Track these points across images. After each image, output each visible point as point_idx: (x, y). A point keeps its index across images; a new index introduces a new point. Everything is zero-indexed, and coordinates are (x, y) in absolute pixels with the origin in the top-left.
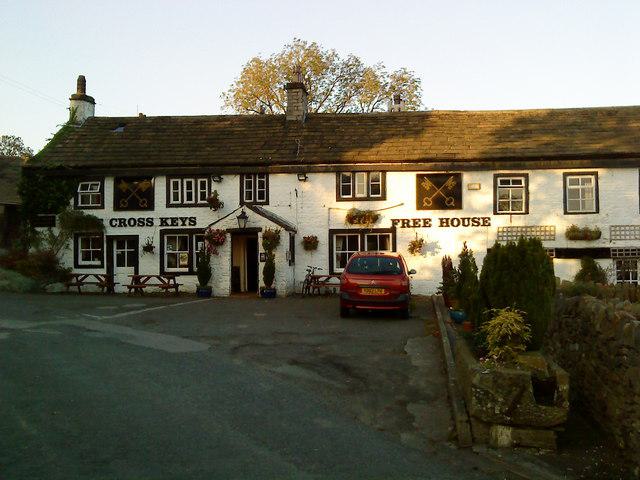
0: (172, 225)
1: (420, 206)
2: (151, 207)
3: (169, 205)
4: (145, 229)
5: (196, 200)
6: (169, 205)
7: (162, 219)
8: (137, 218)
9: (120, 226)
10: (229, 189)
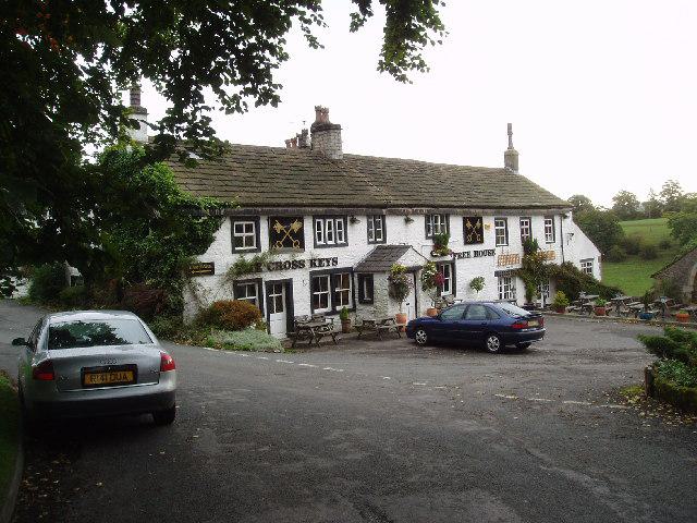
1: (466, 243)
2: (302, 246)
3: (316, 246)
4: (297, 270)
6: (316, 246)
10: (358, 232)
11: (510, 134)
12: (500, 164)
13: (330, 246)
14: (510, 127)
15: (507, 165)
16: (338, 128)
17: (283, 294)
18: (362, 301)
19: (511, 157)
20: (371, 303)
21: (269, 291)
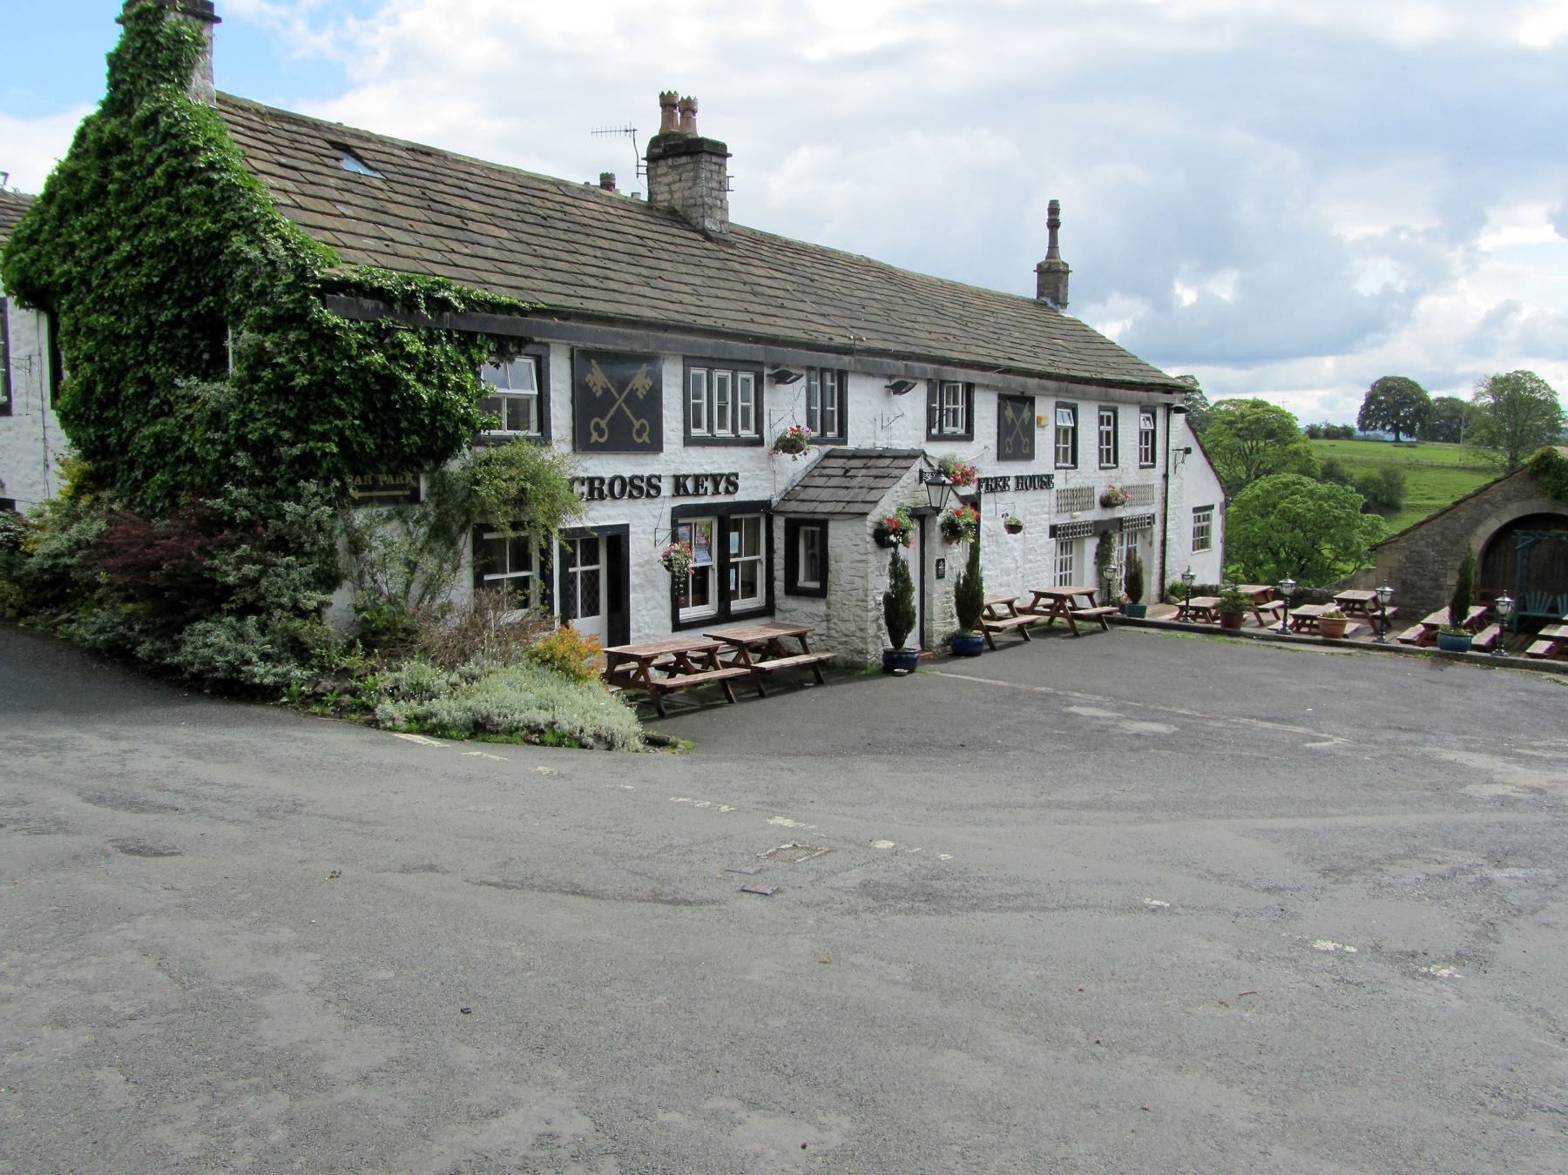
0: (696, 493)
2: (655, 445)
3: (689, 441)
5: (710, 428)
6: (689, 441)
7: (677, 478)
8: (627, 474)
9: (591, 497)
11: (1053, 225)
12: (1027, 288)
13: (725, 442)
14: (1054, 209)
15: (1040, 294)
16: (718, 151)
17: (602, 567)
18: (792, 589)
19: (1052, 276)
20: (821, 593)
21: (567, 560)
